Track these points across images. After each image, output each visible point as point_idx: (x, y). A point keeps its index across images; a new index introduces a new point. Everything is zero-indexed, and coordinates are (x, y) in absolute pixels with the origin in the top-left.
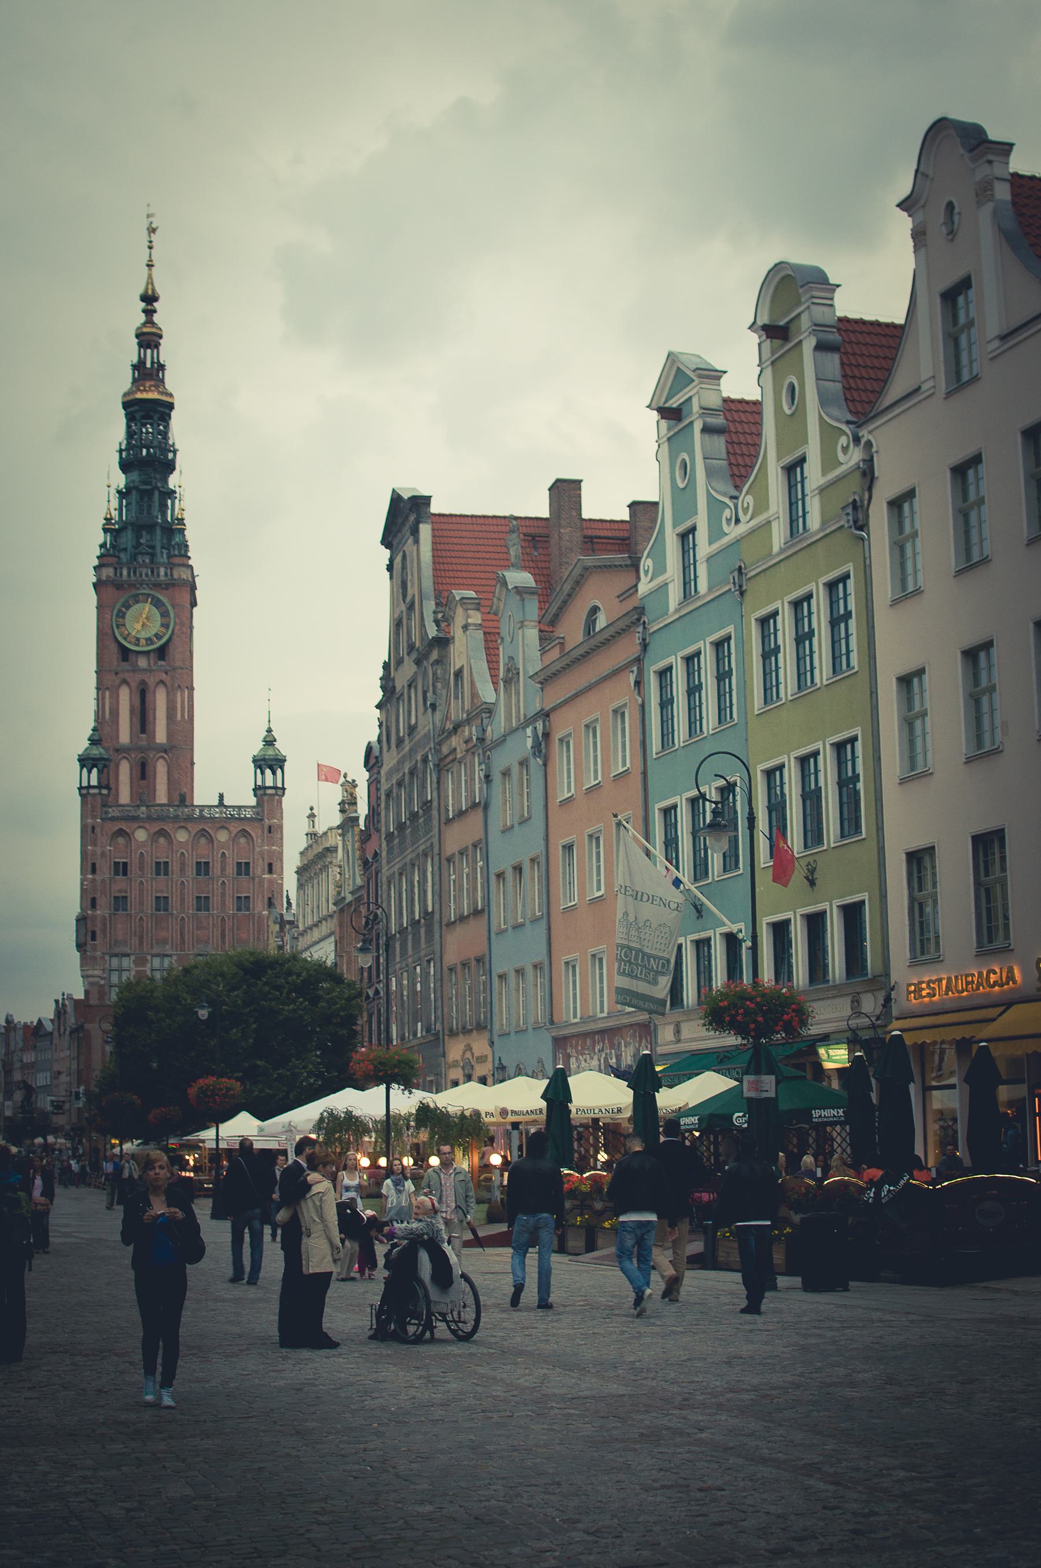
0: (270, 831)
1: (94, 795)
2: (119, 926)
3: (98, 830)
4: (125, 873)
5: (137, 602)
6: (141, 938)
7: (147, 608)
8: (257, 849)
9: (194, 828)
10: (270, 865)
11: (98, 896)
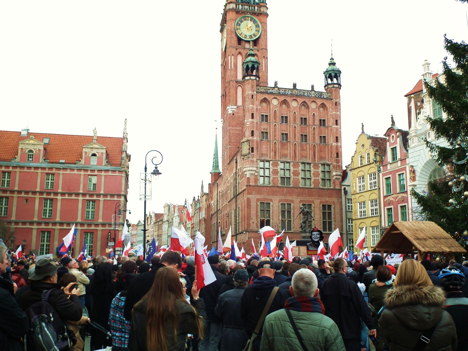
0: (336, 105)
1: (253, 80)
2: (264, 146)
3: (254, 97)
4: (267, 121)
5: (246, 20)
6: (275, 152)
7: (250, 24)
8: (330, 113)
9: (300, 100)
10: (337, 121)
11: (255, 130)
